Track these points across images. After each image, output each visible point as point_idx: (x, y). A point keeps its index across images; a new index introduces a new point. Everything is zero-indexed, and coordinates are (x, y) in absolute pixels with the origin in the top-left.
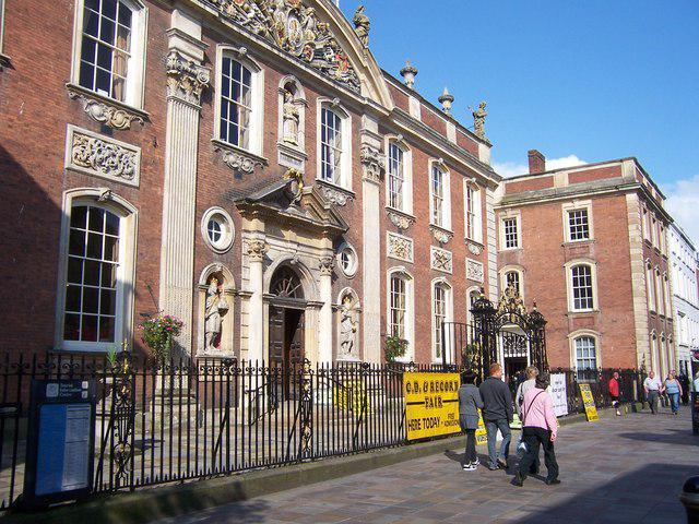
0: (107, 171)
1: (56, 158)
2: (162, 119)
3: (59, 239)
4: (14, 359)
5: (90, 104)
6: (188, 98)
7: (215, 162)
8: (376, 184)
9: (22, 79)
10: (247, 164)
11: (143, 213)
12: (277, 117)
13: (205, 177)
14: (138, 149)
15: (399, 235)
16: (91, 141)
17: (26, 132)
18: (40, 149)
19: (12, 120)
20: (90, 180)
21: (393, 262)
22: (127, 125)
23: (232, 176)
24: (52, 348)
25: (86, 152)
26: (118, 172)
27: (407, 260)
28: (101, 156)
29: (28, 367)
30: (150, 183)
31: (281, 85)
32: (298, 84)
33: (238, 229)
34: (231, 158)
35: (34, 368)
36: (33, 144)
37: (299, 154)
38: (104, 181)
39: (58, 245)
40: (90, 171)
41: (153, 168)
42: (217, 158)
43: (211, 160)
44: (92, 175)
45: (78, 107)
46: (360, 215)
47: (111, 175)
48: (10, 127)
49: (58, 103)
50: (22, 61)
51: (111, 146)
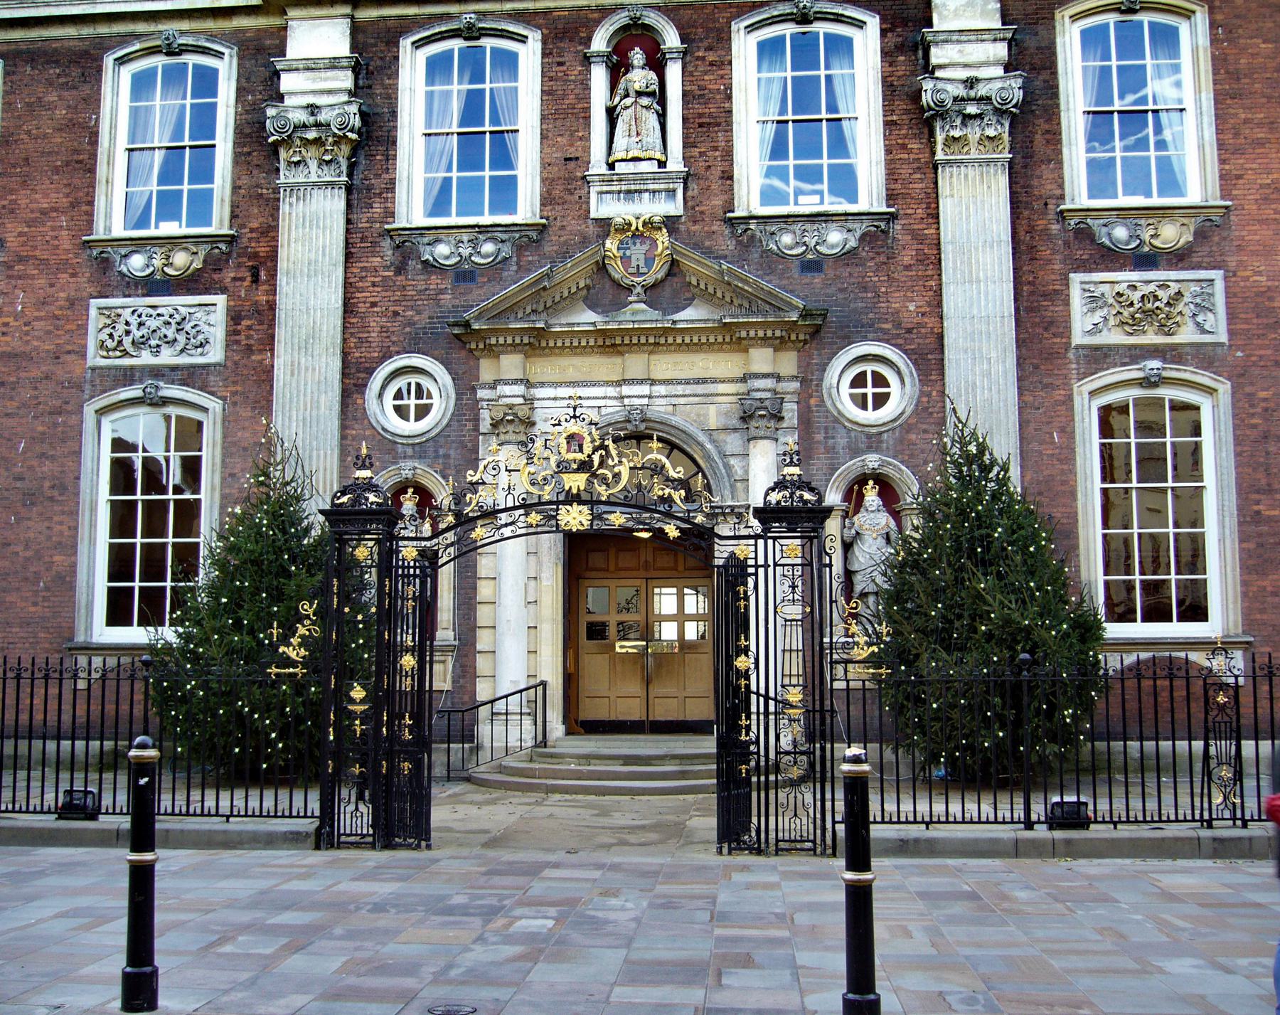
0: (157, 350)
1: (73, 357)
2: (270, 231)
3: (78, 478)
4: (12, 662)
5: (126, 256)
6: (313, 172)
7: (400, 269)
8: (989, 162)
9: (21, 260)
10: (488, 248)
11: (235, 404)
12: (587, 118)
13: (374, 304)
14: (220, 300)
15: (1134, 276)
16: (126, 314)
17: (27, 334)
18: (48, 351)
19: (6, 324)
20: (128, 376)
21: (1098, 357)
22: (198, 264)
23: (447, 284)
24: (71, 639)
25: (116, 335)
26: (179, 348)
27: (1186, 335)
28: (144, 331)
29: (27, 670)
30: (249, 348)
31: (600, 42)
32: (652, 18)
33: (466, 387)
34: (442, 249)
35: (33, 673)
36: (36, 348)
37: (669, 177)
38: (157, 372)
39: (77, 487)
40: (127, 362)
41: (255, 326)
42: (405, 258)
43: (386, 268)
44: (132, 368)
45: (104, 264)
46: (932, 258)
47: (167, 357)
48: (4, 334)
49: (74, 275)
50: (20, 234)
51: (160, 311)
